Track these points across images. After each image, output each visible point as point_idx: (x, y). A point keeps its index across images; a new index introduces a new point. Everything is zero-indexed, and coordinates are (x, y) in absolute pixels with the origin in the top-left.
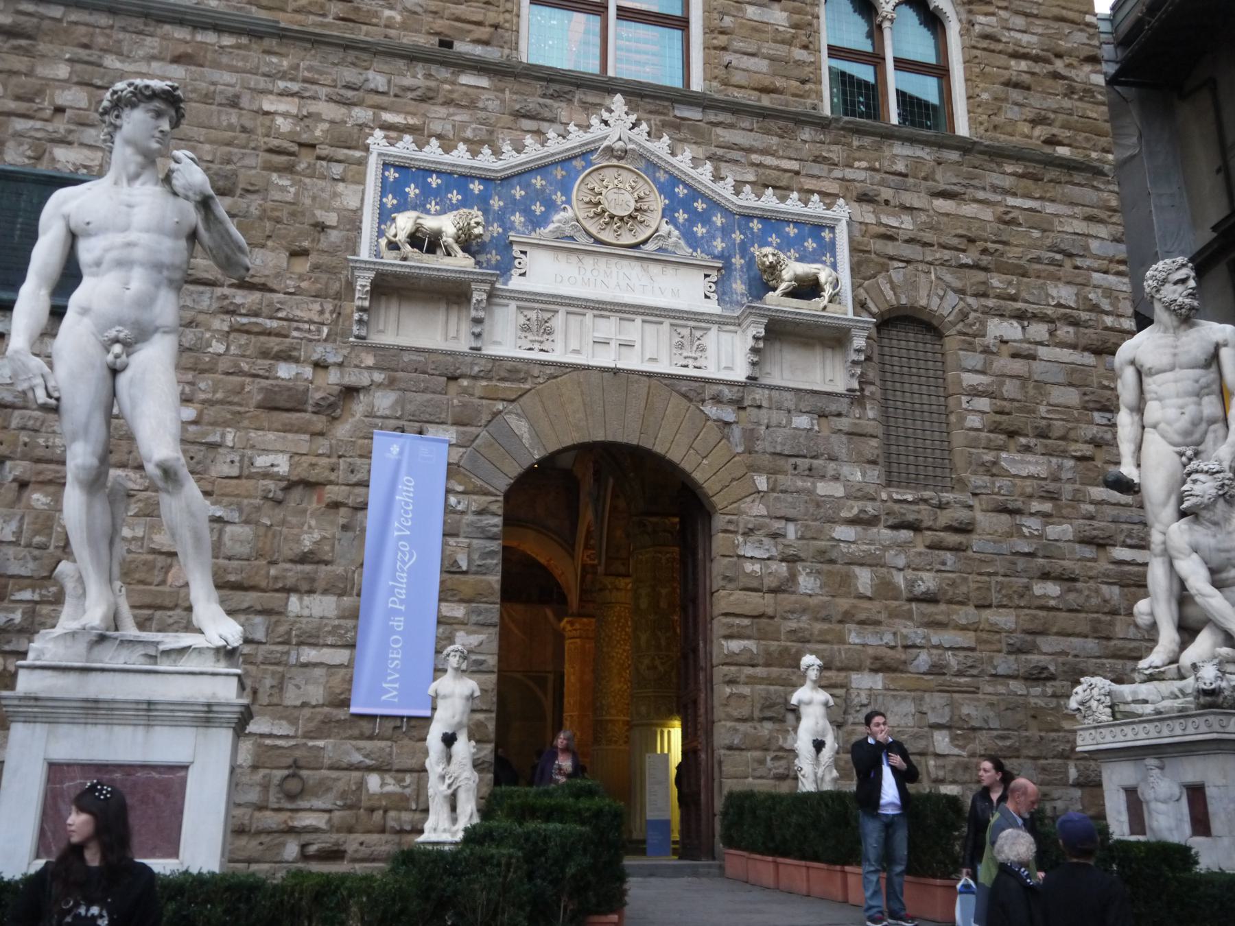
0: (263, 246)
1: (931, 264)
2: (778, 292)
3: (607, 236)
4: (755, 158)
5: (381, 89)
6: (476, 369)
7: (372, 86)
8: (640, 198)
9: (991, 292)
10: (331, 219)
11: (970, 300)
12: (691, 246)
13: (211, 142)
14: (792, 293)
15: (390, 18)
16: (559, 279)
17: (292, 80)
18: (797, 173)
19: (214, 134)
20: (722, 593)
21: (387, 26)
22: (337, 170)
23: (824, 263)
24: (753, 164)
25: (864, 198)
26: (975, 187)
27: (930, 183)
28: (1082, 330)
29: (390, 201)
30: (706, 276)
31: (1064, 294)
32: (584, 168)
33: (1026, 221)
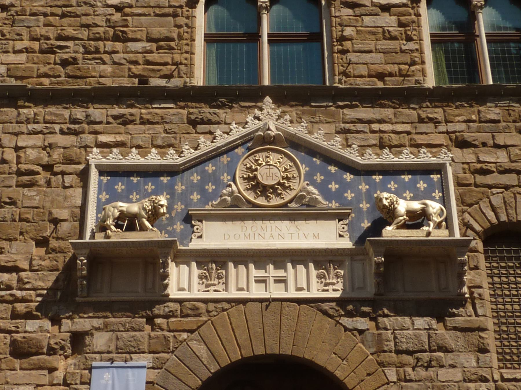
3: (262, 201)
4: (376, 127)
5: (98, 120)
6: (167, 310)
7: (92, 119)
10: (63, 214)
12: (326, 198)
14: (405, 226)
15: (104, 70)
16: (227, 237)
17: (38, 123)
18: (408, 133)
21: (101, 77)
22: (68, 180)
23: (433, 199)
24: (373, 132)
29: (104, 197)
30: (339, 221)
32: (244, 154)
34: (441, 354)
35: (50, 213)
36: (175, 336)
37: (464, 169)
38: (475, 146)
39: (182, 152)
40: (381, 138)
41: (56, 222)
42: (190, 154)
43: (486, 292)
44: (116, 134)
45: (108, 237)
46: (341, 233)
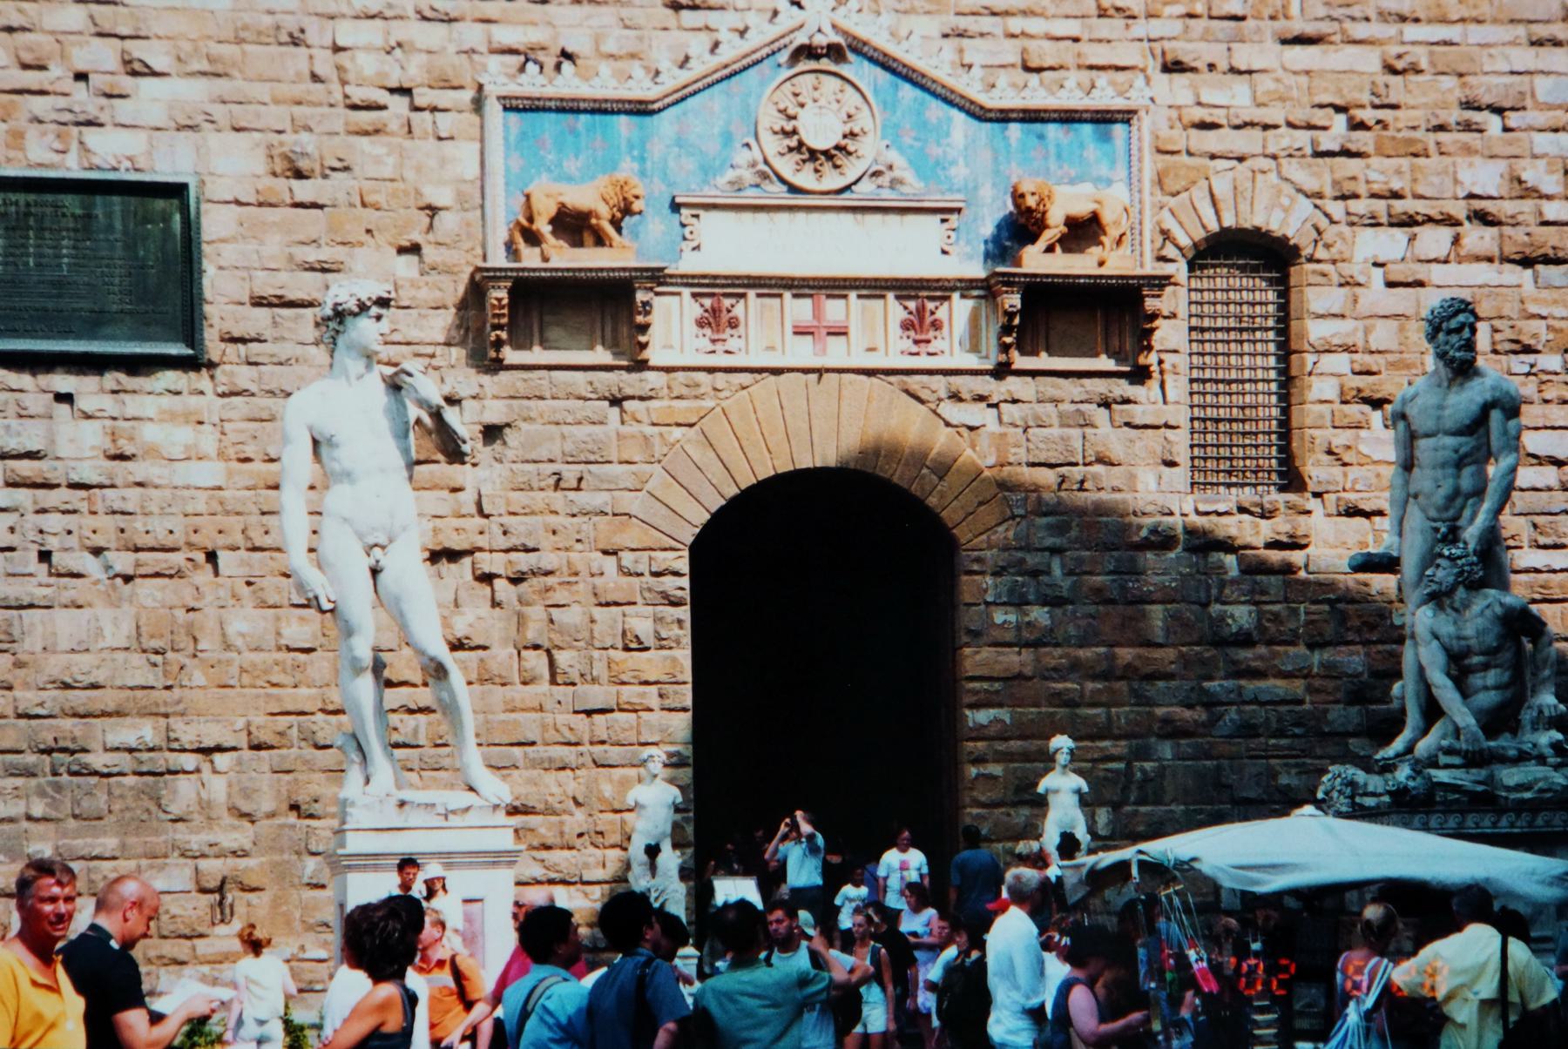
0: (361, 244)
1: (1274, 157)
2: (1042, 243)
3: (805, 179)
4: (1015, 24)
8: (849, 116)
9: (1362, 189)
11: (1337, 209)
13: (277, 102)
19: (285, 90)
20: (967, 651)
22: (445, 123)
25: (1174, 67)
26: (1353, 19)
27: (1277, 25)
28: (1507, 230)
30: (943, 221)
31: (1485, 177)
33: (1432, 64)
34: (1098, 469)
35: (418, 193)
36: (661, 435)
37: (1170, 119)
38: (1193, 70)
39: (657, 73)
40: (1024, 51)
41: (432, 210)
42: (674, 79)
43: (1182, 361)
44: (526, 24)
45: (546, 260)
46: (946, 248)
